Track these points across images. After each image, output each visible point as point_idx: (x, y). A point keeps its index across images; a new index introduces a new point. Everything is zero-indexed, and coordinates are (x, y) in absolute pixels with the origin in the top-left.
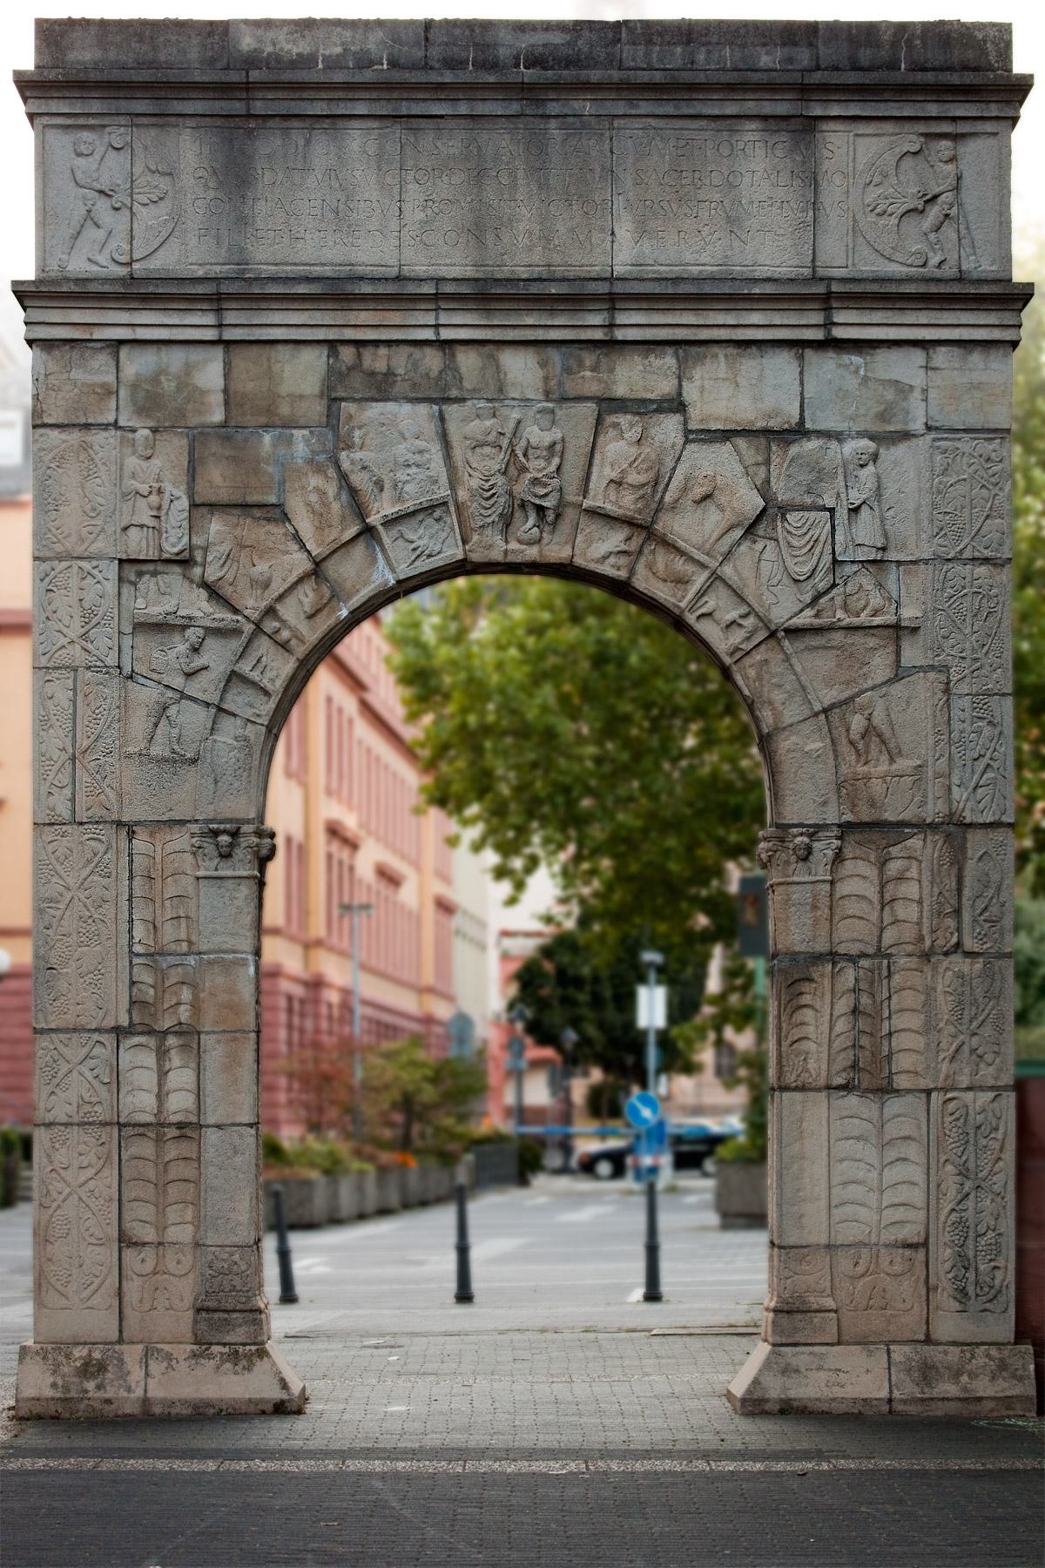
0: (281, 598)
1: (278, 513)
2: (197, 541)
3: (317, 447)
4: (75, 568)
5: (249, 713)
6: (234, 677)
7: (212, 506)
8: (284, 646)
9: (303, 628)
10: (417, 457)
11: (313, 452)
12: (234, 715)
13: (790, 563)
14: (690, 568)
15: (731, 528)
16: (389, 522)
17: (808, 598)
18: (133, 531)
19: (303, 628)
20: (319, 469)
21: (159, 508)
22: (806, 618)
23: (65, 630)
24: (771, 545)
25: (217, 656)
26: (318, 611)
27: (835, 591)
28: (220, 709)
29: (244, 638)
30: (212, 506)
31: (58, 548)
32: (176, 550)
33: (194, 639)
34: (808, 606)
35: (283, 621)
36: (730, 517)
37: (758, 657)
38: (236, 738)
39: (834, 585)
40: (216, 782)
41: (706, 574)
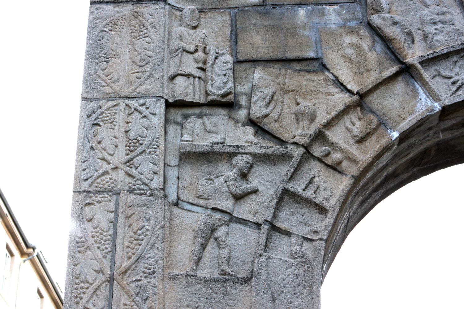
0: (329, 125)
1: (318, 65)
2: (239, 89)
3: (347, 16)
4: (122, 106)
5: (304, 231)
6: (286, 196)
7: (255, 62)
8: (335, 168)
9: (354, 150)
10: (441, 17)
11: (345, 20)
12: (288, 234)
16: (426, 62)
18: (179, 79)
19: (354, 150)
20: (352, 31)
21: (205, 63)
23: (109, 158)
25: (267, 181)
26: (368, 135)
28: (274, 228)
29: (294, 162)
30: (255, 62)
31: (107, 90)
32: (221, 92)
33: (242, 164)
35: (333, 145)
38: (292, 256)
40: (274, 300)
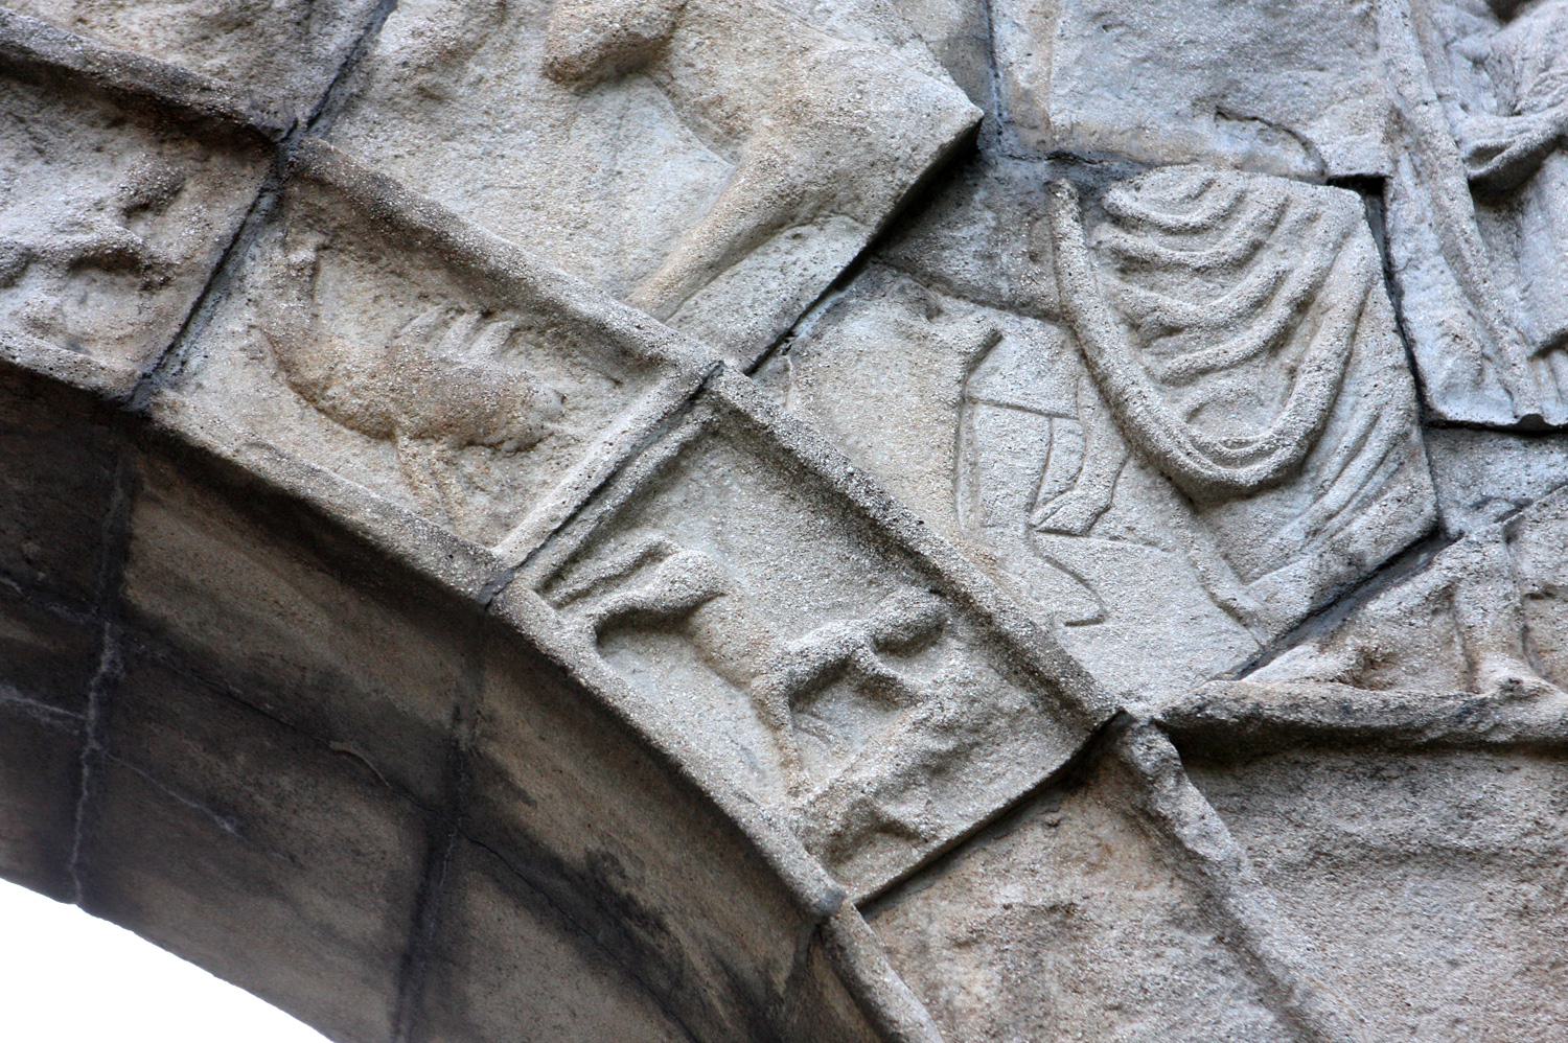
13: (1162, 414)
14: (544, 378)
15: (785, 217)
17: (1291, 589)
22: (1301, 678)
24: (1024, 340)
27: (1446, 564)
34: (1293, 633)
36: (779, 155)
37: (1007, 884)
39: (1435, 536)
41: (650, 400)
